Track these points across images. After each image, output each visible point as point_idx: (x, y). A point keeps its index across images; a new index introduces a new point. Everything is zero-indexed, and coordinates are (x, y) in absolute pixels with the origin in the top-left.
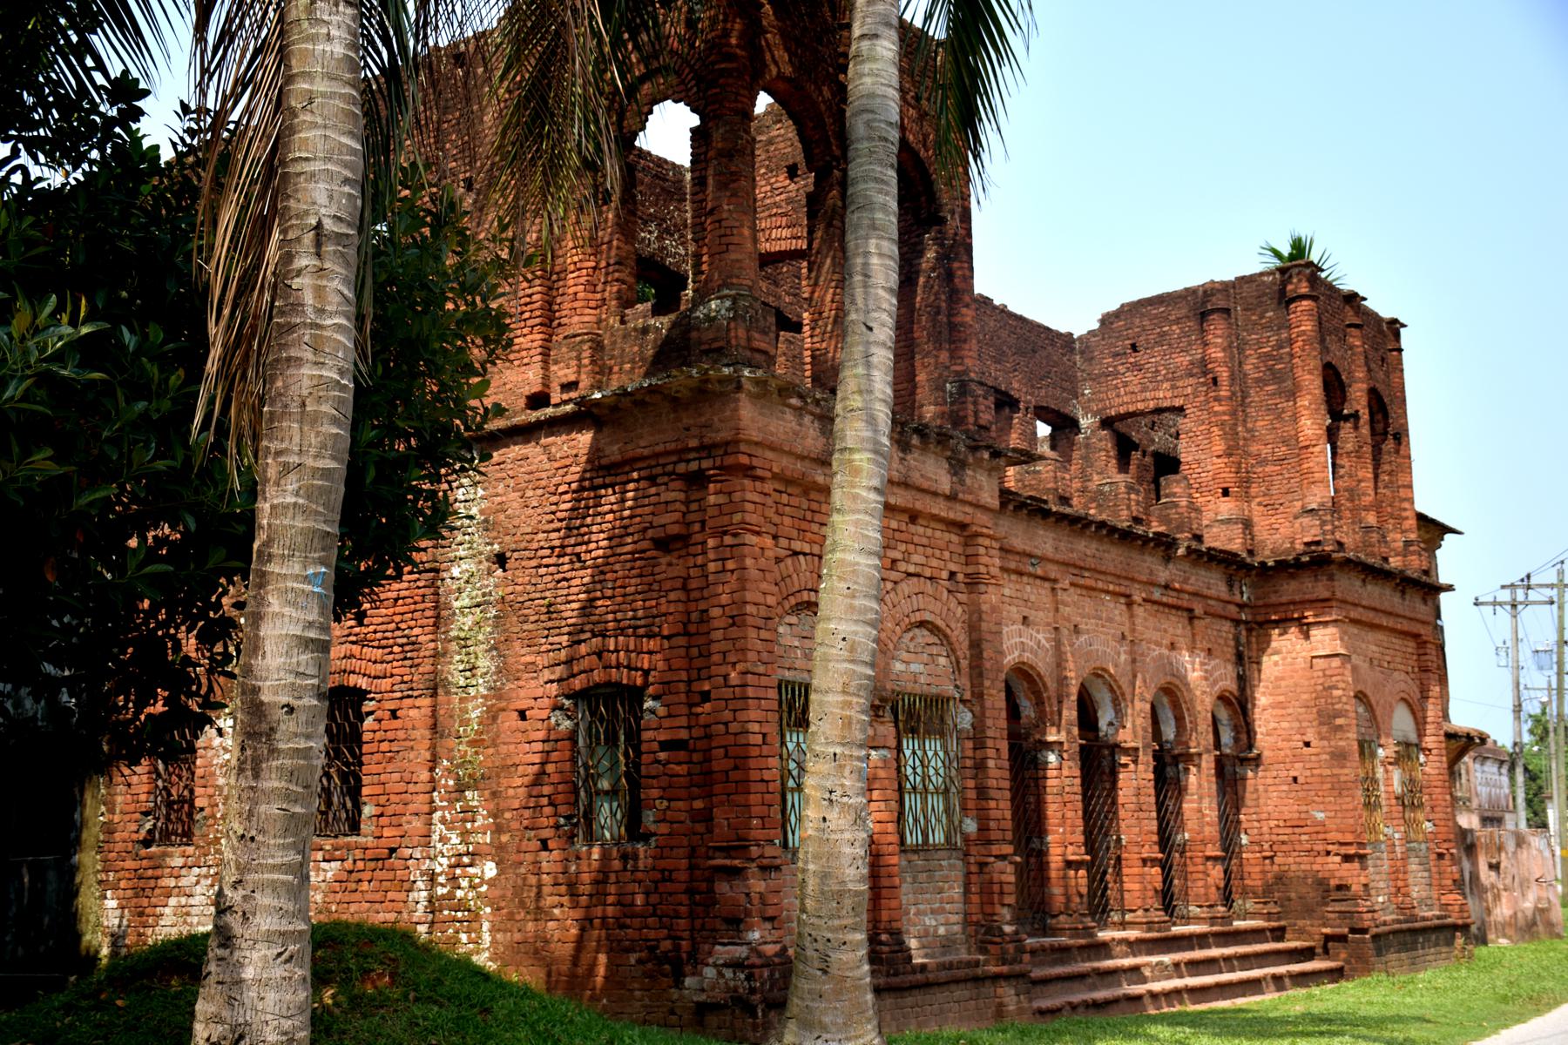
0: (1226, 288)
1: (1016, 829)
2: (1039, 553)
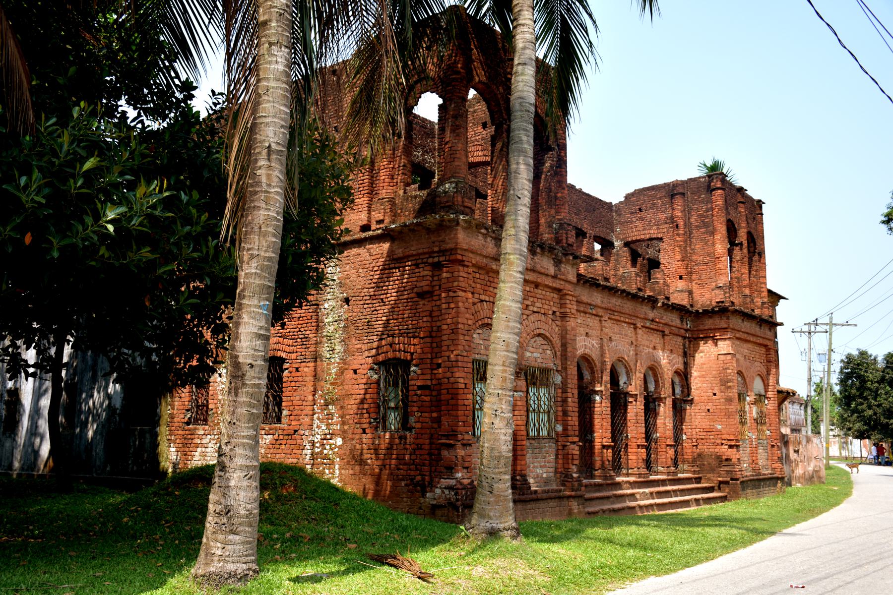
0: (683, 183)
1: (580, 431)
2: (594, 303)
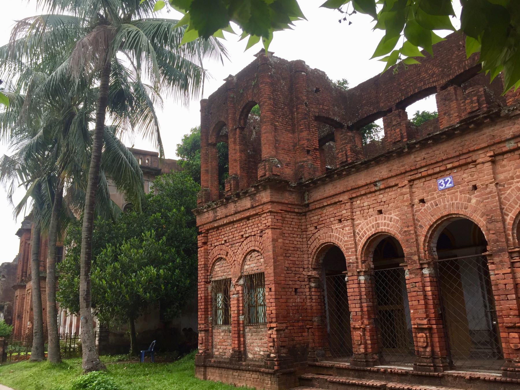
2: (377, 179)
